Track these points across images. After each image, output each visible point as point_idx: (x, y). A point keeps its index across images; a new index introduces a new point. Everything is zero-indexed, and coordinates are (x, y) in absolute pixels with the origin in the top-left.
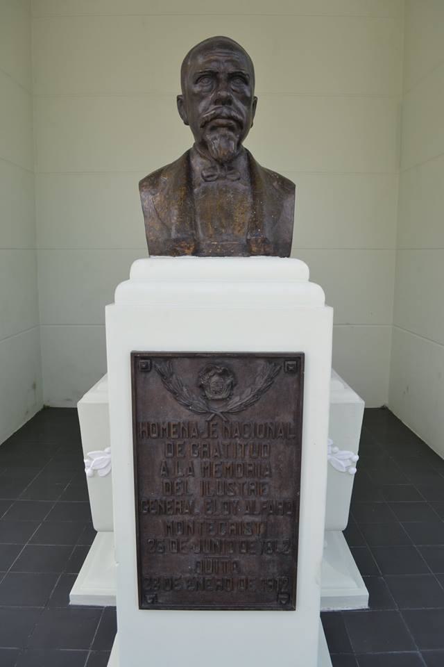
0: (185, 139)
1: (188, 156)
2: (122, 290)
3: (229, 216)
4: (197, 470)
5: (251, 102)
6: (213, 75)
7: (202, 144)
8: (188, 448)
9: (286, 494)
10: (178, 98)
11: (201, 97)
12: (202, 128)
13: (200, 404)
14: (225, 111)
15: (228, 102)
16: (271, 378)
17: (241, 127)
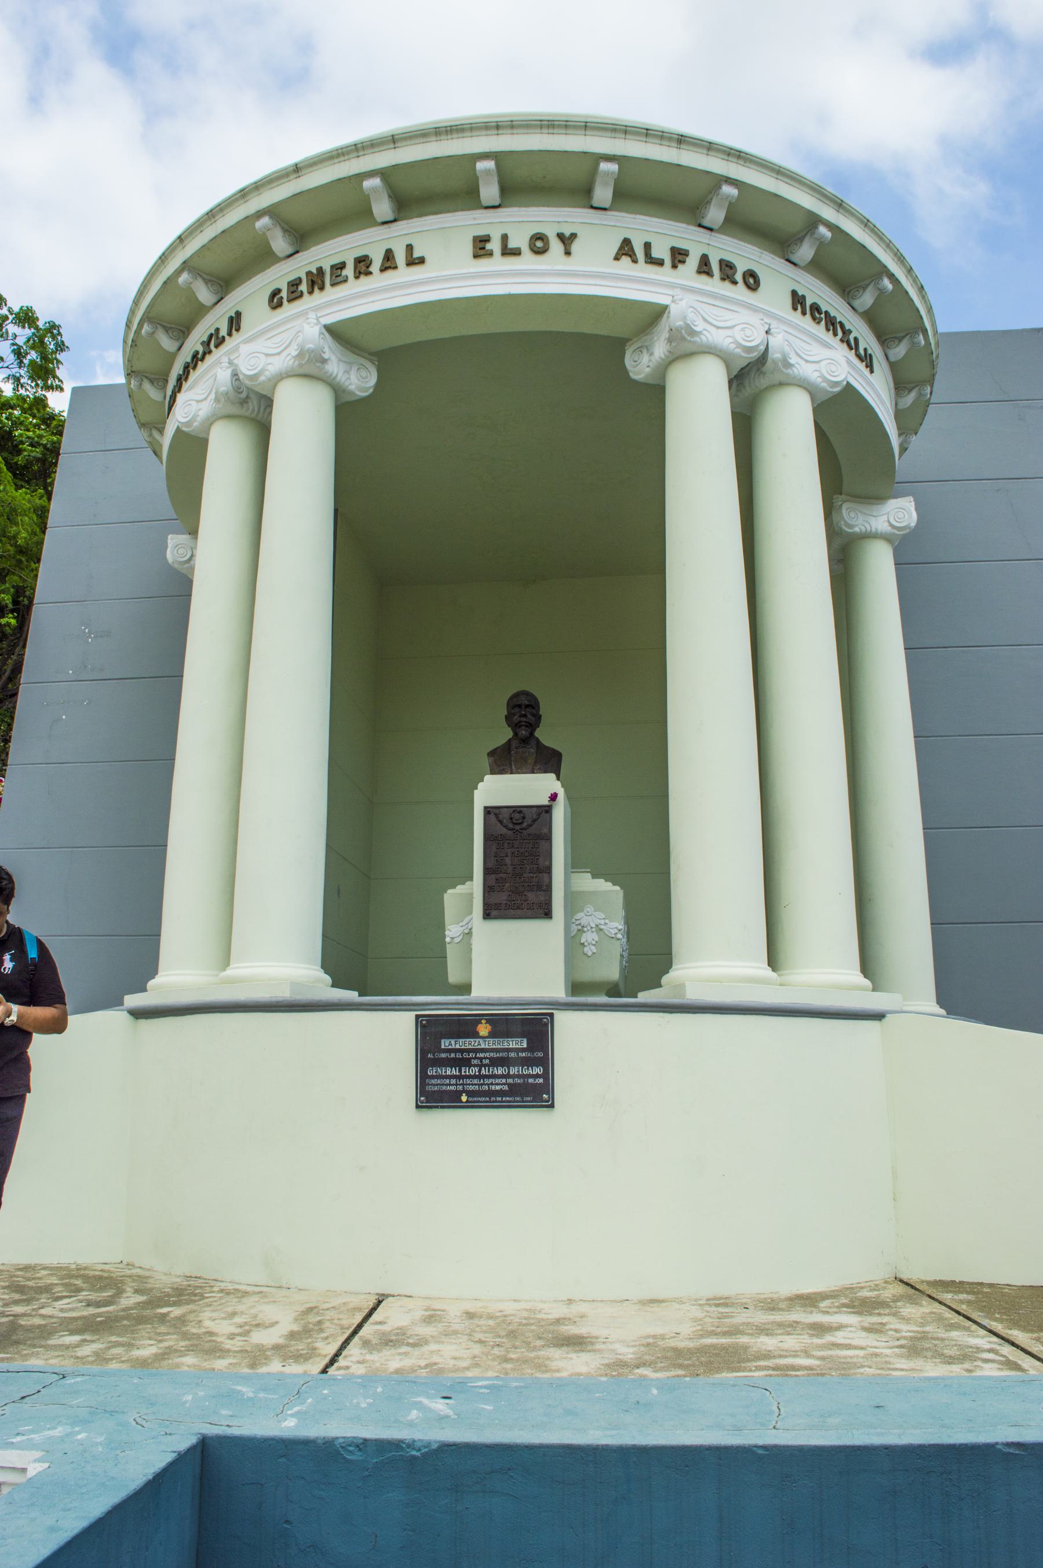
0: (509, 734)
1: (510, 741)
2: (480, 785)
3: (526, 762)
4: (509, 854)
5: (538, 718)
6: (520, 706)
7: (516, 734)
8: (506, 845)
9: (547, 863)
10: (506, 717)
11: (514, 715)
12: (515, 726)
13: (511, 826)
14: (524, 719)
15: (525, 716)
16: (539, 815)
17: (533, 726)
